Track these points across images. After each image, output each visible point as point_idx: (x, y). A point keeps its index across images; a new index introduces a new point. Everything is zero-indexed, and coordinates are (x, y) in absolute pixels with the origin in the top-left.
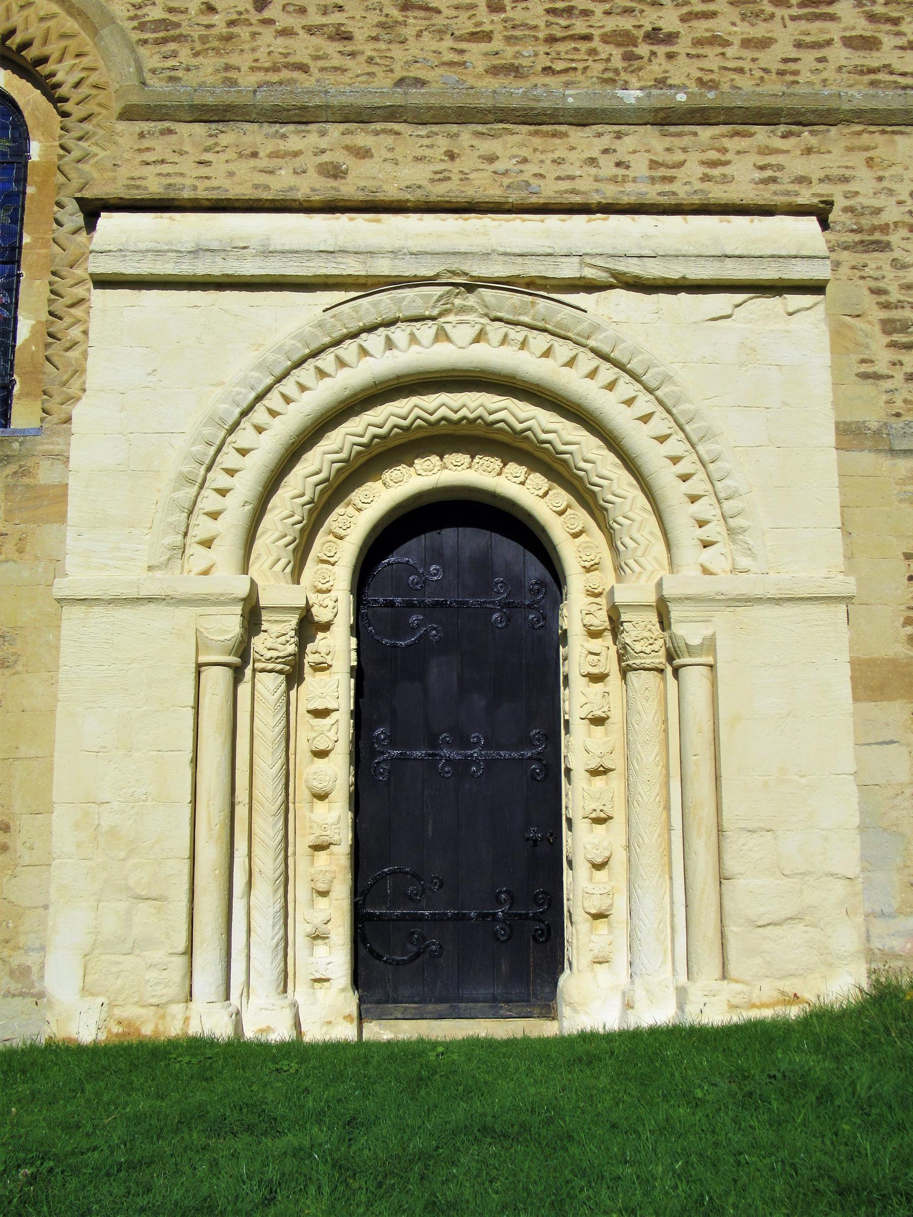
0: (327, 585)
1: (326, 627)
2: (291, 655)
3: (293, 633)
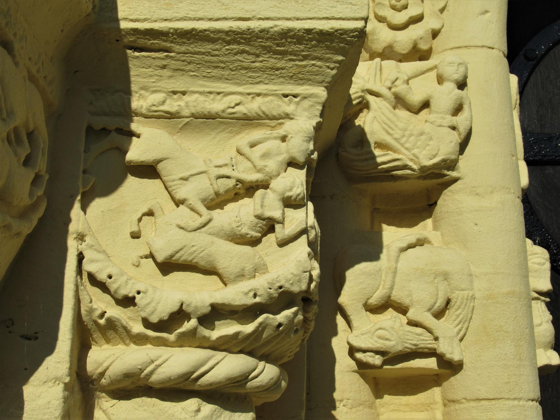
0: (415, 32)
1: (419, 196)
2: (283, 299)
3: (296, 181)
